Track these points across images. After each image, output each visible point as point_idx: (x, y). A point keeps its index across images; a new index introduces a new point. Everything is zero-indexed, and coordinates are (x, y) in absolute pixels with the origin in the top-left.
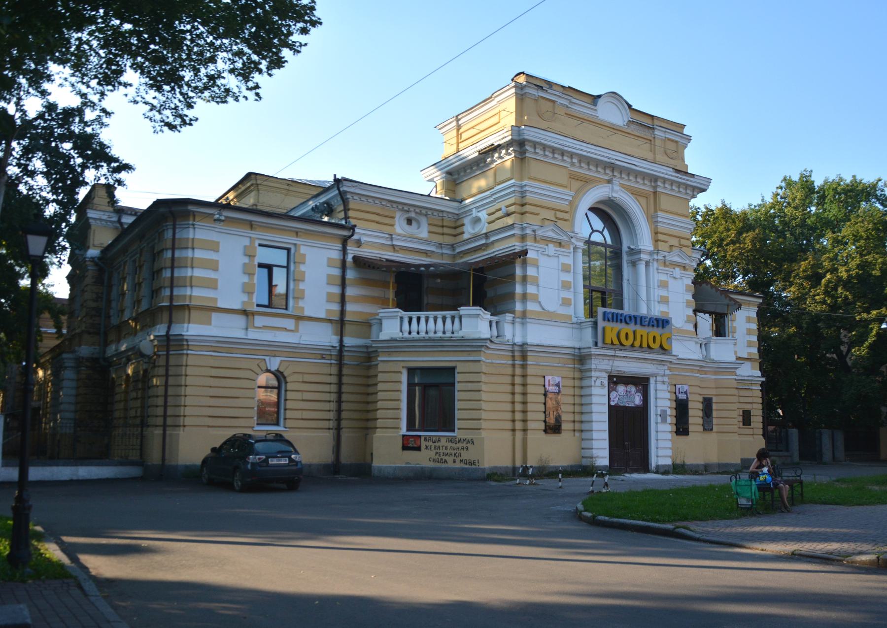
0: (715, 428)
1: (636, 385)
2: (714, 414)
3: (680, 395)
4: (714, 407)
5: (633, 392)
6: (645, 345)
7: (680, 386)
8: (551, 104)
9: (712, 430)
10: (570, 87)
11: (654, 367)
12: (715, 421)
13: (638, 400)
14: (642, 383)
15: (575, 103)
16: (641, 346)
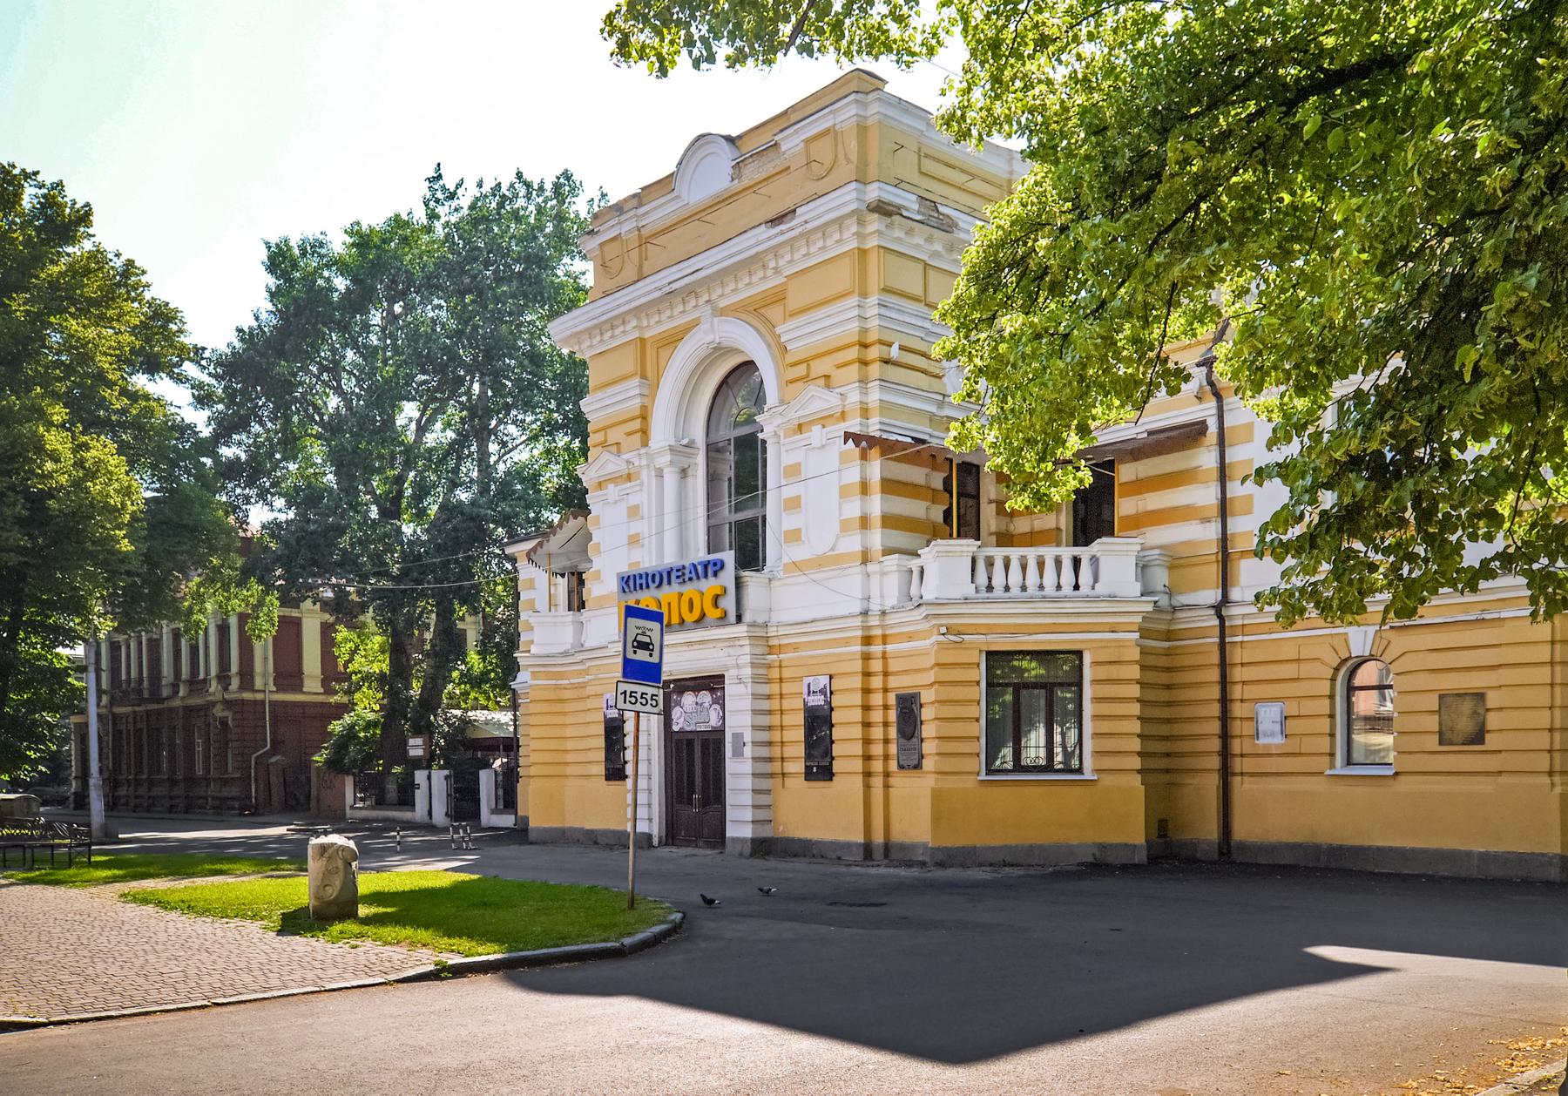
0: (928, 764)
1: (712, 690)
2: (928, 730)
3: (811, 698)
4: (927, 714)
5: (707, 705)
6: (675, 620)
7: (810, 679)
8: (616, 244)
9: (918, 766)
10: (642, 189)
11: (721, 653)
12: (928, 748)
13: (714, 721)
14: (712, 684)
15: (646, 213)
16: (682, 621)
